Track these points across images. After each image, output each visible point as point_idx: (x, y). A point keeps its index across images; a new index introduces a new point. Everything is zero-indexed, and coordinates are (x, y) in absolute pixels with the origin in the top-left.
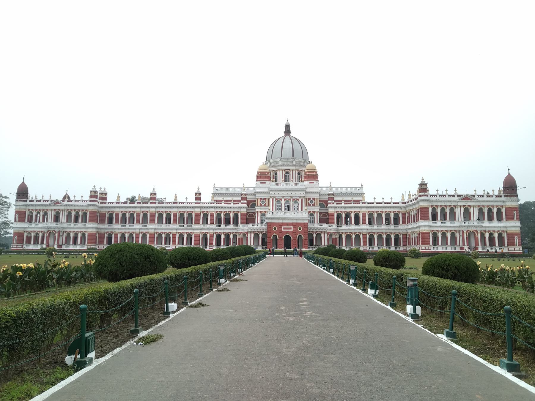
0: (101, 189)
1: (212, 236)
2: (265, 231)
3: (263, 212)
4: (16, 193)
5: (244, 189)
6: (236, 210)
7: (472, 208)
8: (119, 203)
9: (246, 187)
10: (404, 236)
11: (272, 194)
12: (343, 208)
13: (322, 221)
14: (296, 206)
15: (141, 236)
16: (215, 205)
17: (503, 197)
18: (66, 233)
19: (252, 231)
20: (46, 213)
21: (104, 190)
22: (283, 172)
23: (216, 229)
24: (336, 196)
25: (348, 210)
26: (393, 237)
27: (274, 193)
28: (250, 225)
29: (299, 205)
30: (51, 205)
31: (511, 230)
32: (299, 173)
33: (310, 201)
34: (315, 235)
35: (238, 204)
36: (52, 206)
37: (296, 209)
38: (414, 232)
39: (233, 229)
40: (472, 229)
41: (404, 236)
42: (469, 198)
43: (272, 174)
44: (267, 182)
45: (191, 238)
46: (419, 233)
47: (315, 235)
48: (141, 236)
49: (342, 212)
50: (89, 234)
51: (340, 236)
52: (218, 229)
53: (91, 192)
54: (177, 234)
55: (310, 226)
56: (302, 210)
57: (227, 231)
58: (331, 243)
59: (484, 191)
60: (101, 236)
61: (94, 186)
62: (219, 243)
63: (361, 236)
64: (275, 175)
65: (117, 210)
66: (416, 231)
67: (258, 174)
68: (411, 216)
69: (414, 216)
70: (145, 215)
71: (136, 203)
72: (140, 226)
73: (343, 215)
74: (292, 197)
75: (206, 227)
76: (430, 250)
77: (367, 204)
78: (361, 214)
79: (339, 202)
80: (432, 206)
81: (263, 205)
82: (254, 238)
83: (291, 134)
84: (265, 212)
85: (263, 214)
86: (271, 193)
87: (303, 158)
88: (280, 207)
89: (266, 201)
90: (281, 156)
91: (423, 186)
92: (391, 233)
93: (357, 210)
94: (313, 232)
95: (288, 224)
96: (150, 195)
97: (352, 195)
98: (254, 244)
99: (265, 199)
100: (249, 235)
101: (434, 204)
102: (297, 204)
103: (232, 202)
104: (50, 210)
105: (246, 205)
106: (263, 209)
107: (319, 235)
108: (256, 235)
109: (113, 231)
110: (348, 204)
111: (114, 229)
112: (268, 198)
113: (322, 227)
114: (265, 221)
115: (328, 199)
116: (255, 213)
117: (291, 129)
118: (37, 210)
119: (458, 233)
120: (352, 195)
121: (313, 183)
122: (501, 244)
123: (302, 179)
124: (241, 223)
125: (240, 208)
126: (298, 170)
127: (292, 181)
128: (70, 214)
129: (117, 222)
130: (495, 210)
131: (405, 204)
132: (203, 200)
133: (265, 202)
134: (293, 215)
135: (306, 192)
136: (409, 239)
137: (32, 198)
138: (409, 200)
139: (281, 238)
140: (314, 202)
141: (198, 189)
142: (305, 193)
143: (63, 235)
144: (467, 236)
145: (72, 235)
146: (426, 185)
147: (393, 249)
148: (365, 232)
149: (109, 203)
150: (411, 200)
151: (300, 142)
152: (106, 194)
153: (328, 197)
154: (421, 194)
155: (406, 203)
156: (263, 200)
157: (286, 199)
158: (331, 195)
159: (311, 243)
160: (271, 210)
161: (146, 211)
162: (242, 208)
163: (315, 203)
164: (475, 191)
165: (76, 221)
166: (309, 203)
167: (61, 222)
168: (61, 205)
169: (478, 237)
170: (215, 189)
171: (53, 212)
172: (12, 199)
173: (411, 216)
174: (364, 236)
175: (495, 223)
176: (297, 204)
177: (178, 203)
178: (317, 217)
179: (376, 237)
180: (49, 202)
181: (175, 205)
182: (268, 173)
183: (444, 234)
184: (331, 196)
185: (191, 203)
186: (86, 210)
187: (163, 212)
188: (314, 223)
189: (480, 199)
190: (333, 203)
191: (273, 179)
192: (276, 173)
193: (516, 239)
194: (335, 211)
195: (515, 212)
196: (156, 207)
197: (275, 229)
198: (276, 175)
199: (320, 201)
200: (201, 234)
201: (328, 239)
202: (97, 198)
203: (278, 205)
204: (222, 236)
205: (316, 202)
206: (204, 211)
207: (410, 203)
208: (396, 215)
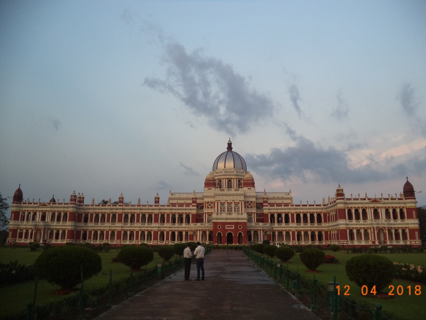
0: (79, 194)
1: (168, 233)
2: (211, 229)
3: (210, 213)
4: (13, 197)
5: (195, 194)
6: (188, 211)
7: (380, 209)
8: (93, 205)
9: (196, 193)
10: (326, 233)
11: (218, 198)
12: (275, 210)
13: (258, 221)
14: (237, 208)
15: (110, 232)
16: (171, 207)
17: (404, 199)
18: (50, 230)
19: (201, 229)
20: (35, 214)
21: (82, 194)
22: (226, 180)
23: (171, 227)
24: (269, 199)
25: (279, 211)
26: (317, 233)
27: (219, 198)
28: (199, 224)
29: (239, 207)
30: (40, 207)
31: (411, 226)
32: (239, 181)
33: (248, 204)
34: (252, 233)
35: (189, 206)
36: (40, 207)
37: (237, 211)
38: (334, 229)
39: (185, 228)
40: (381, 226)
41: (326, 233)
42: (377, 200)
43: (217, 181)
44: (213, 189)
45: (151, 235)
46: (338, 230)
47: (252, 233)
48: (110, 232)
49: (274, 213)
50: (68, 231)
51: (274, 233)
52: (173, 227)
53: (71, 196)
54: (140, 232)
55: (249, 224)
56: (242, 212)
57: (180, 229)
58: (266, 239)
59: (389, 195)
60: (78, 232)
61: (74, 192)
63: (291, 233)
64: (220, 182)
65: (91, 211)
66: (336, 229)
67: (205, 181)
68: (331, 216)
69: (333, 216)
70: (114, 215)
71: (107, 206)
72: (109, 224)
73: (276, 216)
74: (233, 201)
75: (163, 226)
76: (348, 244)
77: (294, 206)
78: (290, 214)
79: (272, 205)
80: (348, 208)
81: (210, 207)
82: (202, 235)
83: (233, 150)
84: (212, 213)
85: (210, 214)
86: (216, 198)
87: (242, 169)
88: (224, 209)
89: (212, 204)
90: (225, 168)
91: (339, 191)
92: (315, 230)
93: (287, 211)
94: (251, 230)
95: (230, 223)
96: (119, 199)
97: (282, 199)
98: (202, 240)
99: (211, 202)
100: (198, 232)
101: (350, 206)
102: (238, 206)
103: (177, 204)
104: (39, 210)
105: (196, 207)
106: (210, 211)
107: (256, 232)
108: (204, 232)
109: (88, 228)
110: (279, 206)
111: (88, 227)
112: (214, 201)
113: (259, 225)
114: (211, 220)
115: (263, 202)
116: (203, 214)
117: (232, 146)
119: (370, 230)
120: (282, 198)
121: (251, 189)
122: (405, 238)
123: (241, 186)
124: (192, 222)
125: (191, 210)
126: (239, 178)
127: (234, 187)
128: (54, 214)
129: (91, 221)
130: (398, 211)
131: (326, 206)
132: (161, 203)
133: (211, 205)
134: (234, 215)
135: (245, 197)
136: (330, 235)
137: (25, 201)
138: (329, 202)
139: (224, 235)
140: (252, 205)
141: (158, 194)
142: (244, 197)
143: (48, 231)
144: (377, 232)
145: (55, 232)
146: (342, 190)
147: (317, 243)
148: (294, 229)
149: (85, 205)
150: (330, 202)
151: (239, 156)
152: (83, 198)
153: (263, 201)
154: (339, 197)
155: (327, 205)
156: (210, 203)
157: (229, 202)
158: (265, 199)
159: (250, 239)
160: (216, 211)
161: (115, 212)
162: (193, 210)
163: (252, 205)
164: (382, 195)
165: (59, 220)
166: (247, 205)
167: (46, 221)
168: (46, 207)
169: (386, 233)
170: (171, 194)
171: (41, 212)
172: (10, 201)
173: (331, 216)
174: (293, 233)
175: (399, 221)
176: (238, 206)
177: (141, 206)
178: (254, 217)
179: (303, 233)
180: (39, 204)
181: (139, 207)
182: (214, 181)
183: (358, 231)
184: (265, 200)
185: (152, 206)
186: (67, 211)
187: (128, 213)
188: (252, 222)
189: (386, 201)
190: (267, 206)
191: (218, 186)
192: (221, 181)
193: (416, 234)
194: (269, 212)
196: (123, 209)
197: (219, 227)
198: (221, 183)
199: (256, 204)
200: (159, 232)
201: (264, 235)
202: (76, 201)
203: (222, 207)
204: (176, 233)
205: (253, 205)
206: (162, 213)
207: (329, 205)
208: (319, 215)
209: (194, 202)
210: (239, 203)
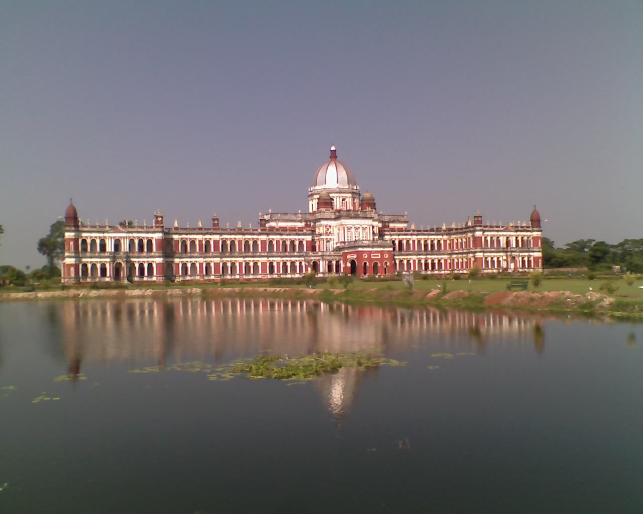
62: (272, 272)
79: (393, 230)
99: (330, 226)
104: (109, 237)
118: (92, 237)
128: (132, 242)
156: (328, 227)
190: (388, 231)
195: (539, 240)
209: (307, 226)
210: (367, 228)
